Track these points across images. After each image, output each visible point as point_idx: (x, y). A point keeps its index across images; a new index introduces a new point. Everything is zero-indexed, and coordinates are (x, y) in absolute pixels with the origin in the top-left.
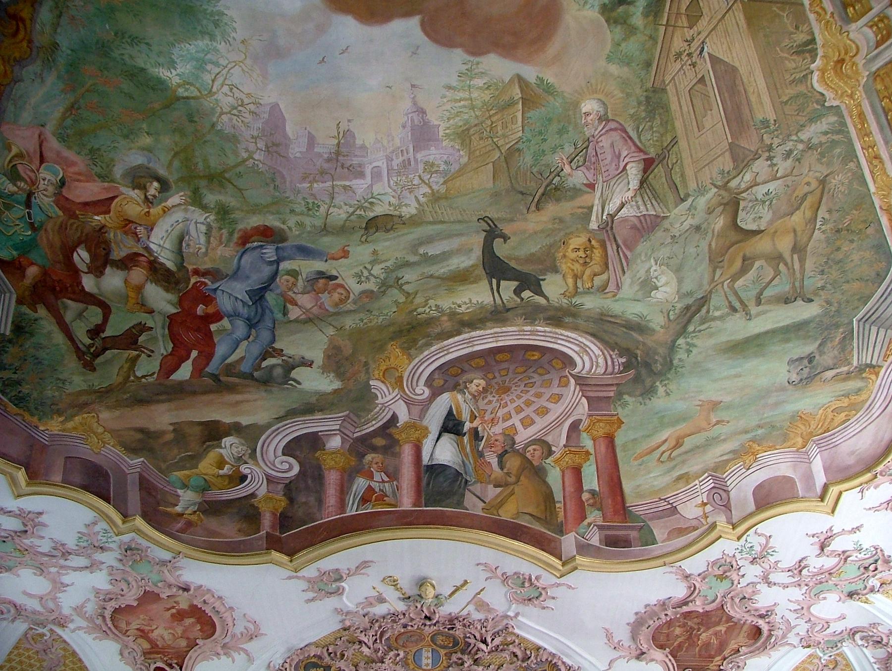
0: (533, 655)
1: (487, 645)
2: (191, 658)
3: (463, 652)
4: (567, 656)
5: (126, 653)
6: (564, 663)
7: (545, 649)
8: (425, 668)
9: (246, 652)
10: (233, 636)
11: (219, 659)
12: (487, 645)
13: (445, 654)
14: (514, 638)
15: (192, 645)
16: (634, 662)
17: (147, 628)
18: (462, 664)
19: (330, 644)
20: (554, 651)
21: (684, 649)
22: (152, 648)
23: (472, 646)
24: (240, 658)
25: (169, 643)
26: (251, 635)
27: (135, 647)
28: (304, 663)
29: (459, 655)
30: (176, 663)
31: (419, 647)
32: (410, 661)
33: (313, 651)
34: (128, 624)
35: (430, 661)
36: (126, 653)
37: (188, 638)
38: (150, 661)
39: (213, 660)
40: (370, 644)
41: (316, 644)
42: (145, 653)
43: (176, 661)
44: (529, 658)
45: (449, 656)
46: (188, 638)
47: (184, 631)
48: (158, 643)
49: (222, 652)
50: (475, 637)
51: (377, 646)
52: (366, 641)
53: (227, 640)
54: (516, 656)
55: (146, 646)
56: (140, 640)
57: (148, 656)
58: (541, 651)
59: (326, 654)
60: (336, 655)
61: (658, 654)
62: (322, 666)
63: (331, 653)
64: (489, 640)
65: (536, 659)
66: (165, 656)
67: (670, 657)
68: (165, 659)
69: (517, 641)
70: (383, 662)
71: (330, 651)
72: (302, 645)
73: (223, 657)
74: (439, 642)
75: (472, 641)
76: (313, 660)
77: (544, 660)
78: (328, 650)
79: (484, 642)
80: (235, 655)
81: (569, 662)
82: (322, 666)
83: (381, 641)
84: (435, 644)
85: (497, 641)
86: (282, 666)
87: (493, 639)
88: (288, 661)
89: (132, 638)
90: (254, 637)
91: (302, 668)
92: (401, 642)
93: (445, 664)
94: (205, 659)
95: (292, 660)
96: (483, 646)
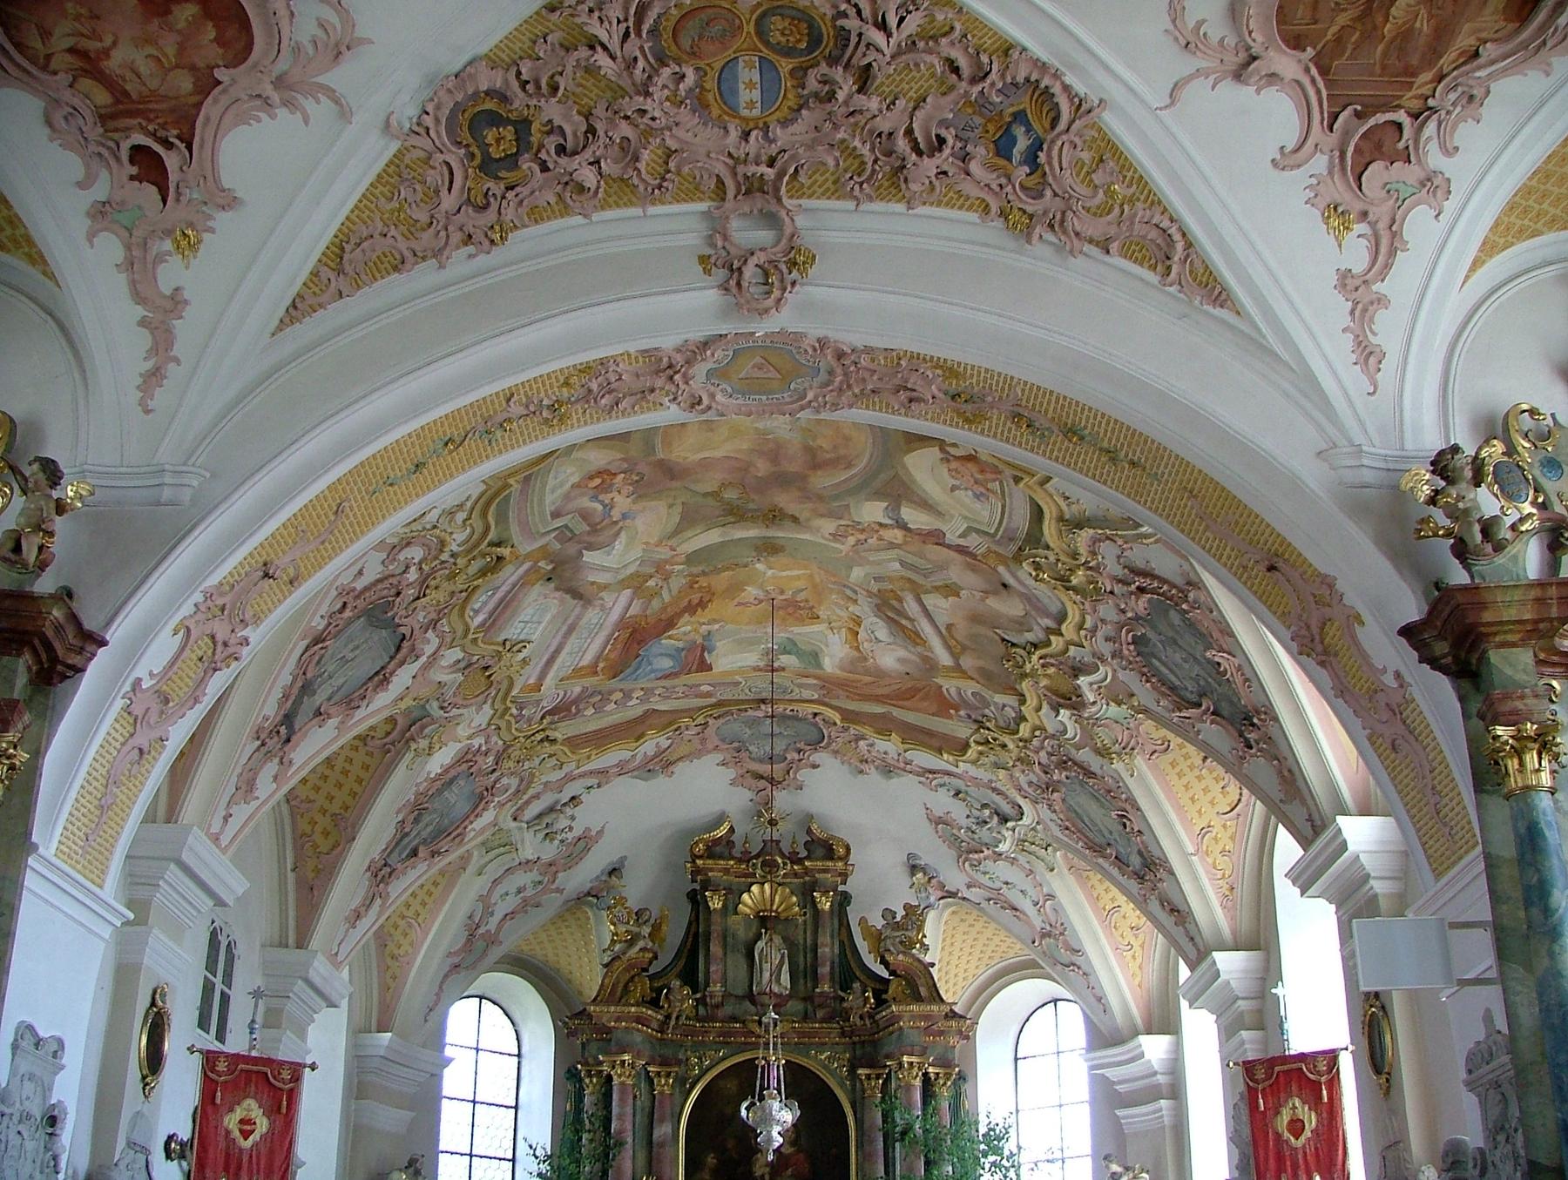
0: (995, 67)
1: (889, 35)
2: (208, 119)
3: (833, 61)
4: (1074, 67)
5: (58, 118)
6: (1066, 88)
7: (1024, 49)
8: (745, 113)
9: (330, 93)
10: (297, 49)
11: (273, 117)
12: (889, 35)
13: (792, 72)
14: (950, 16)
15: (207, 85)
16: (1228, 88)
17: (92, 45)
18: (831, 96)
19: (521, 58)
20: (1044, 57)
21: (1350, 47)
22: (118, 102)
23: (854, 39)
24: (319, 109)
25: (153, 84)
26: (337, 45)
27: (76, 102)
28: (466, 116)
29: (824, 68)
30: (179, 137)
31: (730, 54)
32: (710, 97)
33: (486, 80)
34: (45, 34)
35: (756, 94)
36: (58, 118)
37: (193, 68)
38: (116, 136)
39: (259, 120)
40: (614, 45)
41: (492, 61)
42: (104, 118)
43: (175, 132)
44: (988, 74)
45: (799, 74)
46: (193, 68)
47: (182, 48)
48: (128, 87)
49: (275, 98)
50: (859, 12)
51: (633, 47)
52: (604, 37)
53: (283, 65)
54: (956, 70)
55: (103, 97)
56: (86, 83)
57: (111, 124)
58: (1015, 54)
59: (515, 85)
60: (538, 87)
61: (1288, 64)
62: (508, 121)
63: (528, 82)
64: (892, 21)
65: (1003, 77)
66: (150, 121)
67: (1314, 71)
68: (151, 128)
69: (958, 26)
70: (647, 94)
71: (524, 77)
72: (458, 66)
73: (282, 113)
74: (776, 37)
75: (852, 24)
76: (489, 105)
77: (1020, 79)
78: (519, 73)
79: (882, 26)
80: (309, 104)
81: (1080, 88)
82: (508, 121)
83: (639, 34)
84: (767, 44)
85: (913, 23)
86: (419, 124)
87: (902, 20)
88: (430, 109)
89: (63, 78)
90: (343, 49)
91: (465, 129)
92: (686, 43)
93: (792, 101)
94: (243, 120)
95: (438, 107)
96: (878, 37)
